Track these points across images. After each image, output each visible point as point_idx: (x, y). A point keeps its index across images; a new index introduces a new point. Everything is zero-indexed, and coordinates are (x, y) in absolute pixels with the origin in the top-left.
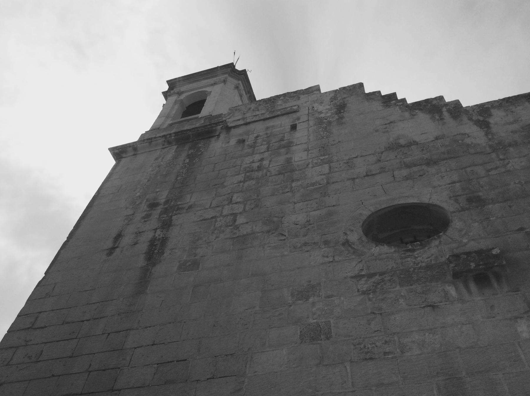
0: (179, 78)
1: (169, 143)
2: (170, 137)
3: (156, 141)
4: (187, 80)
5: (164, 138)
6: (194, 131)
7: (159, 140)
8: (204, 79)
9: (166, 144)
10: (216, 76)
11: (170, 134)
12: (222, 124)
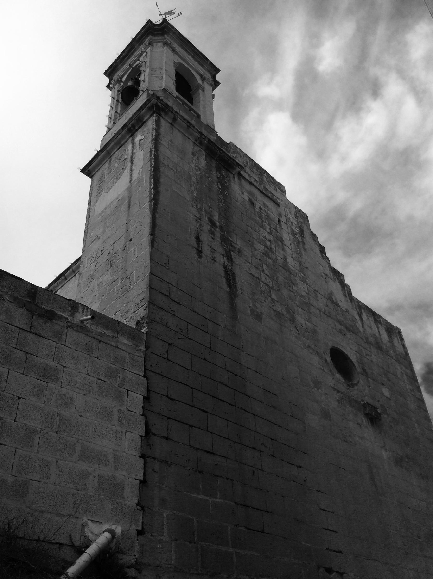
1: (201, 143)
2: (203, 138)
4: (178, 39)
6: (222, 154)
7: (196, 132)
8: (193, 57)
9: (198, 141)
10: (202, 66)
11: (206, 137)
12: (240, 168)
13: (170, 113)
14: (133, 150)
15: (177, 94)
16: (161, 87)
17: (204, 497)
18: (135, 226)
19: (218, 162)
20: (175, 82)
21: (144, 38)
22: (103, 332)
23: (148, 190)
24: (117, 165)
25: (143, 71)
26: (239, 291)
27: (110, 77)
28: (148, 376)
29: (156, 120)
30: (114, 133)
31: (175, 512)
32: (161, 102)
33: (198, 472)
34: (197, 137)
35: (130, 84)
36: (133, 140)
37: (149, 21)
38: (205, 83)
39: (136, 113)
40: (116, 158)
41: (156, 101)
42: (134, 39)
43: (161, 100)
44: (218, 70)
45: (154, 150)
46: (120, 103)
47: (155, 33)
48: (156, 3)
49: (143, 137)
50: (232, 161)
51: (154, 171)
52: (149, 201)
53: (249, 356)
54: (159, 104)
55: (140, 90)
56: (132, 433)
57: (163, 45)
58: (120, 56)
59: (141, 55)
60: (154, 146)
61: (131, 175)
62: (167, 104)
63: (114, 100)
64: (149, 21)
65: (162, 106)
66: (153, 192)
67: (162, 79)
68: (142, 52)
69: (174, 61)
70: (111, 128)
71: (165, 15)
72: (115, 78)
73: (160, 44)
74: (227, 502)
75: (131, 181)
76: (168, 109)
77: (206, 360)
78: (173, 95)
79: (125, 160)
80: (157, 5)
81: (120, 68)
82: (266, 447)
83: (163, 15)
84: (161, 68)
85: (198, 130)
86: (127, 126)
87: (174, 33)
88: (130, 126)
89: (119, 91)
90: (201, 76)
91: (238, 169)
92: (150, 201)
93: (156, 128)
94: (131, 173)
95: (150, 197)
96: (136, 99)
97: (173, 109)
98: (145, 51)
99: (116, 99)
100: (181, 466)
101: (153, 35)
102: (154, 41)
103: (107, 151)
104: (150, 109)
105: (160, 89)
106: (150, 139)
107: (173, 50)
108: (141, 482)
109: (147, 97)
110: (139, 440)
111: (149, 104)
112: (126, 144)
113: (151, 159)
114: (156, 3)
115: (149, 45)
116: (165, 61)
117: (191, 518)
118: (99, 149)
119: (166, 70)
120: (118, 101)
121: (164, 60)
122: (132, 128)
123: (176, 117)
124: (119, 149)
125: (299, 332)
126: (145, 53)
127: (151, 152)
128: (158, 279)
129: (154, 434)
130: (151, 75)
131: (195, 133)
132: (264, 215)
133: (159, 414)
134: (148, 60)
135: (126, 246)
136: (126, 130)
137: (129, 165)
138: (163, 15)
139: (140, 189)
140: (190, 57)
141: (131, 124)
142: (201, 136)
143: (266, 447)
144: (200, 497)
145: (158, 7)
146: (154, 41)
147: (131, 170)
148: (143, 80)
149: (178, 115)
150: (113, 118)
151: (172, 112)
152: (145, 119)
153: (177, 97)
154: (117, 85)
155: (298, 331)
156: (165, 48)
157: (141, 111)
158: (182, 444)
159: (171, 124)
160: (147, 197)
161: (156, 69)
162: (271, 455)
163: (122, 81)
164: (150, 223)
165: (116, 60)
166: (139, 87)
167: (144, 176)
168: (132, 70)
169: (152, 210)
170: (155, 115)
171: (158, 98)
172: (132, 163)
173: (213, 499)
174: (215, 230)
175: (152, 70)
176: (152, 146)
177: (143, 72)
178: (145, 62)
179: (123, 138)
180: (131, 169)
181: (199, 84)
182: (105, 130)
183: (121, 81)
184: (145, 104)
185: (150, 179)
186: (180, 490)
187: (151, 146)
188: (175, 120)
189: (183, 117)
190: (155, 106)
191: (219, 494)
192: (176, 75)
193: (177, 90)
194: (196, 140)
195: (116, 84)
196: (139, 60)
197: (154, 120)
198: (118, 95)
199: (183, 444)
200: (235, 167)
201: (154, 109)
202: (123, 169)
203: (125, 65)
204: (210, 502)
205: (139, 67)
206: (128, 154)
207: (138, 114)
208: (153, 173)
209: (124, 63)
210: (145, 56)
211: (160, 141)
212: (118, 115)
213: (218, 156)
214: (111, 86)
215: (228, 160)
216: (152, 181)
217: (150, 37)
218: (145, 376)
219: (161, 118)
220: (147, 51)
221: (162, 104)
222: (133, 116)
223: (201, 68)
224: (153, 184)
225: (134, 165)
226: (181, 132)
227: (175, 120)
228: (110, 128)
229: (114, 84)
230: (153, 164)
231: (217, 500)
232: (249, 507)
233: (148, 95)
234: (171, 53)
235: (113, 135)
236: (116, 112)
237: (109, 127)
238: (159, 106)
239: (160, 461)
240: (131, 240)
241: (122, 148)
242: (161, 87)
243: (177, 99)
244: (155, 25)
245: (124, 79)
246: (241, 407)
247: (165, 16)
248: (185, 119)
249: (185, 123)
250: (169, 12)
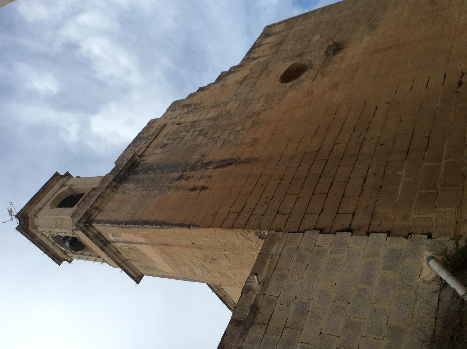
0: (24, 207)
1: (115, 187)
2: (112, 185)
3: (105, 194)
5: (108, 188)
6: (124, 170)
7: (107, 191)
8: (46, 193)
9: (114, 189)
10: (53, 186)
11: (110, 183)
12: (136, 155)
13: (91, 212)
14: (121, 242)
15: (76, 206)
16: (70, 219)
17: (401, 185)
18: (182, 240)
19: (131, 173)
20: (66, 208)
21: (31, 233)
22: (268, 266)
23: (153, 229)
24: (134, 255)
25: (57, 233)
26: (235, 156)
27: (62, 260)
28: (303, 230)
29: (96, 223)
30: (108, 257)
31: (413, 208)
32: (82, 219)
33: (380, 190)
34: (110, 190)
35: (67, 244)
36: (113, 242)
37: (17, 229)
38: (67, 184)
39: (91, 239)
40: (128, 256)
41: (81, 223)
42: (32, 241)
43: (81, 219)
44: (57, 174)
45: (120, 225)
46: (83, 252)
47: (26, 224)
48: (2, 223)
49: (110, 234)
50: (130, 162)
51: (138, 225)
52: (162, 229)
53: (287, 148)
54: (84, 221)
55: (73, 236)
56: (349, 243)
57: (36, 217)
58: (45, 253)
59: (44, 235)
60: (118, 225)
61: (141, 243)
62: (84, 215)
63: (80, 257)
64: (17, 229)
65: (85, 218)
66: (155, 226)
67: (64, 219)
68: (42, 234)
69: (49, 209)
70: (104, 259)
71: (12, 216)
72: (63, 256)
73: (36, 220)
74: (405, 166)
75: (146, 244)
76: (88, 213)
77: (291, 183)
78: (76, 209)
79: (129, 248)
80: (4, 223)
81: (55, 252)
82: (360, 135)
83: (12, 217)
84: (55, 219)
85: (105, 190)
86: (102, 246)
87: (27, 209)
88: (102, 245)
89: (73, 253)
90: (61, 187)
91: (137, 157)
92: (162, 228)
93: (103, 223)
94: (139, 244)
95: (159, 228)
96: (80, 239)
97: (88, 210)
98: (41, 232)
99: (80, 255)
100: (376, 203)
101: (28, 225)
102: (33, 225)
103: (122, 262)
104: (88, 228)
105: (72, 220)
106: (113, 228)
107: (40, 209)
108: (389, 235)
109: (78, 230)
110: (355, 237)
111: (84, 229)
112: (116, 247)
113: (129, 227)
114: (2, 223)
115: (36, 229)
116: (49, 216)
117: (417, 195)
118: (120, 269)
119: (57, 215)
120: (81, 254)
121: (48, 216)
122: (104, 243)
123: (94, 207)
124: (120, 253)
125: (268, 108)
126: (43, 232)
127: (122, 227)
128: (225, 222)
129: (350, 225)
130: (60, 227)
131: (107, 192)
132: (174, 137)
134: (48, 230)
135: (199, 248)
136: (105, 248)
137: (133, 245)
138: (12, 217)
139: (152, 236)
140: (46, 196)
141: (100, 244)
142: (110, 187)
143: (360, 135)
144: (401, 188)
145: (6, 222)
146: (33, 225)
147: (137, 243)
148: (65, 234)
149: (93, 206)
150: (95, 258)
151: (91, 210)
152: (96, 232)
153: (78, 206)
154: (68, 255)
155: (267, 109)
156: (39, 216)
157: (90, 235)
158: (358, 203)
159: (100, 211)
160: (159, 230)
161: (56, 223)
162: (367, 131)
163: (66, 251)
164: (180, 228)
165: (49, 255)
166: (70, 237)
167: (142, 233)
168: (56, 243)
169: (169, 227)
170: (93, 224)
171: (79, 222)
172: (132, 242)
173: (403, 178)
174: (186, 175)
175: (57, 226)
176: (118, 226)
177: (58, 234)
178: (50, 232)
179: (111, 250)
180: (136, 243)
181: (67, 189)
182: (105, 265)
183: (65, 252)
184: (84, 232)
185: (144, 228)
186: (396, 204)
187: (118, 227)
188: (97, 208)
189: (94, 202)
190: (85, 224)
191: (398, 173)
192: (60, 207)
193: (72, 206)
194: (113, 191)
195: (68, 255)
196: (48, 237)
197: (97, 225)
198: (76, 254)
199: (358, 202)
200: (134, 160)
201: (87, 225)
202: (136, 250)
203: (53, 248)
204: (405, 180)
205: (54, 237)
206: (125, 246)
207: (92, 238)
208: (140, 226)
209: (50, 249)
210: (45, 232)
211: (114, 220)
212: (93, 254)
213: (126, 173)
214: (69, 260)
215: (129, 166)
216: (146, 226)
217: (29, 228)
218: (303, 233)
219: (95, 219)
220: (41, 231)
221: (84, 219)
222: (93, 242)
223: (55, 187)
224: (149, 226)
225: (133, 241)
226: (106, 203)
227: (97, 208)
228: (103, 260)
229: (68, 257)
230: (132, 225)
231: (404, 174)
232: (409, 148)
233: (77, 230)
234: (43, 211)
235: (109, 257)
236: (90, 255)
237: (103, 261)
238: (86, 221)
239: (372, 220)
240: (194, 244)
241: (120, 251)
242: (70, 219)
243: (80, 206)
244: (20, 225)
245: (64, 249)
246: (328, 155)
247: (13, 216)
248: (96, 200)
249: (99, 200)
250: (9, 213)
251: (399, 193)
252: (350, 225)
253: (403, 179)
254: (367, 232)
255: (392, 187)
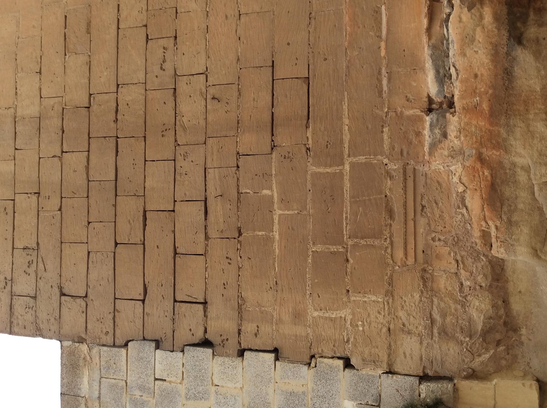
17: (276, 227)
74: (274, 172)
100: (239, 275)
108: (277, 359)
110: (219, 360)
129: (206, 331)
133: (174, 319)
144: (277, 237)
158: (207, 273)
173: (276, 206)
186: (275, 280)
199: (206, 271)
204: (281, 212)
251: (277, 251)
252: (206, 331)
253: (278, 212)
254: (239, 350)
255: (260, 233)
